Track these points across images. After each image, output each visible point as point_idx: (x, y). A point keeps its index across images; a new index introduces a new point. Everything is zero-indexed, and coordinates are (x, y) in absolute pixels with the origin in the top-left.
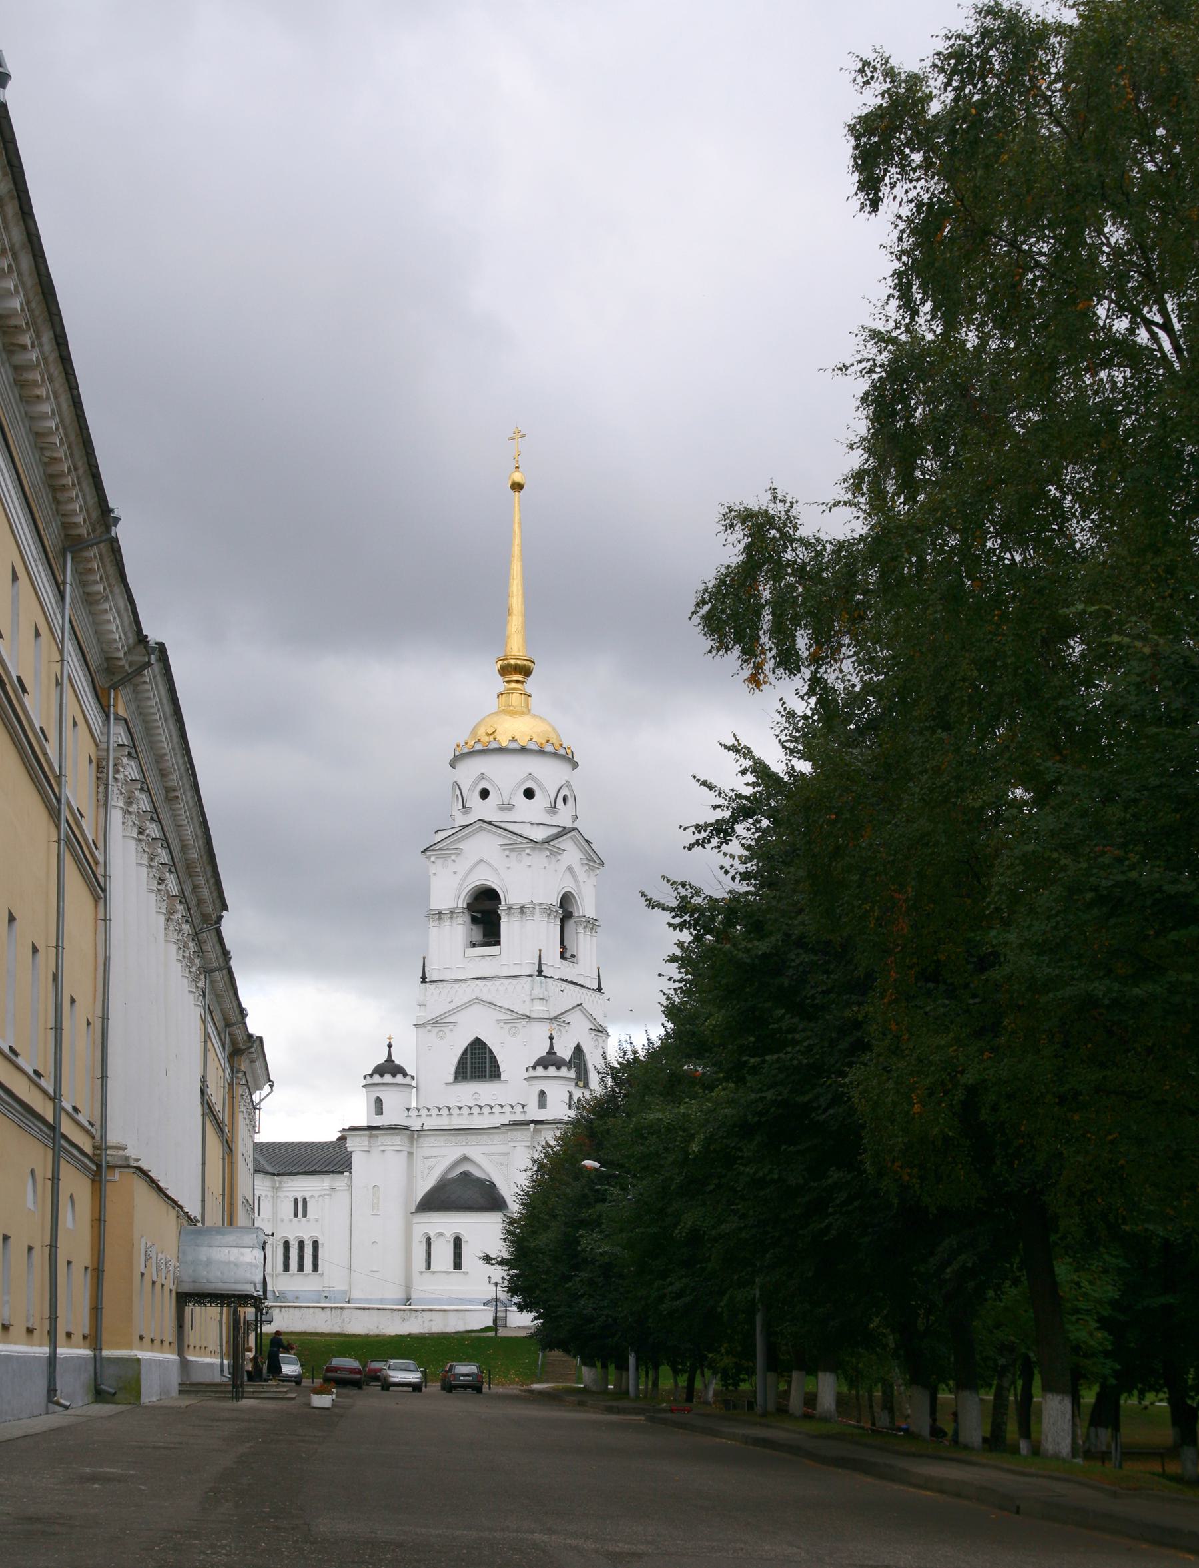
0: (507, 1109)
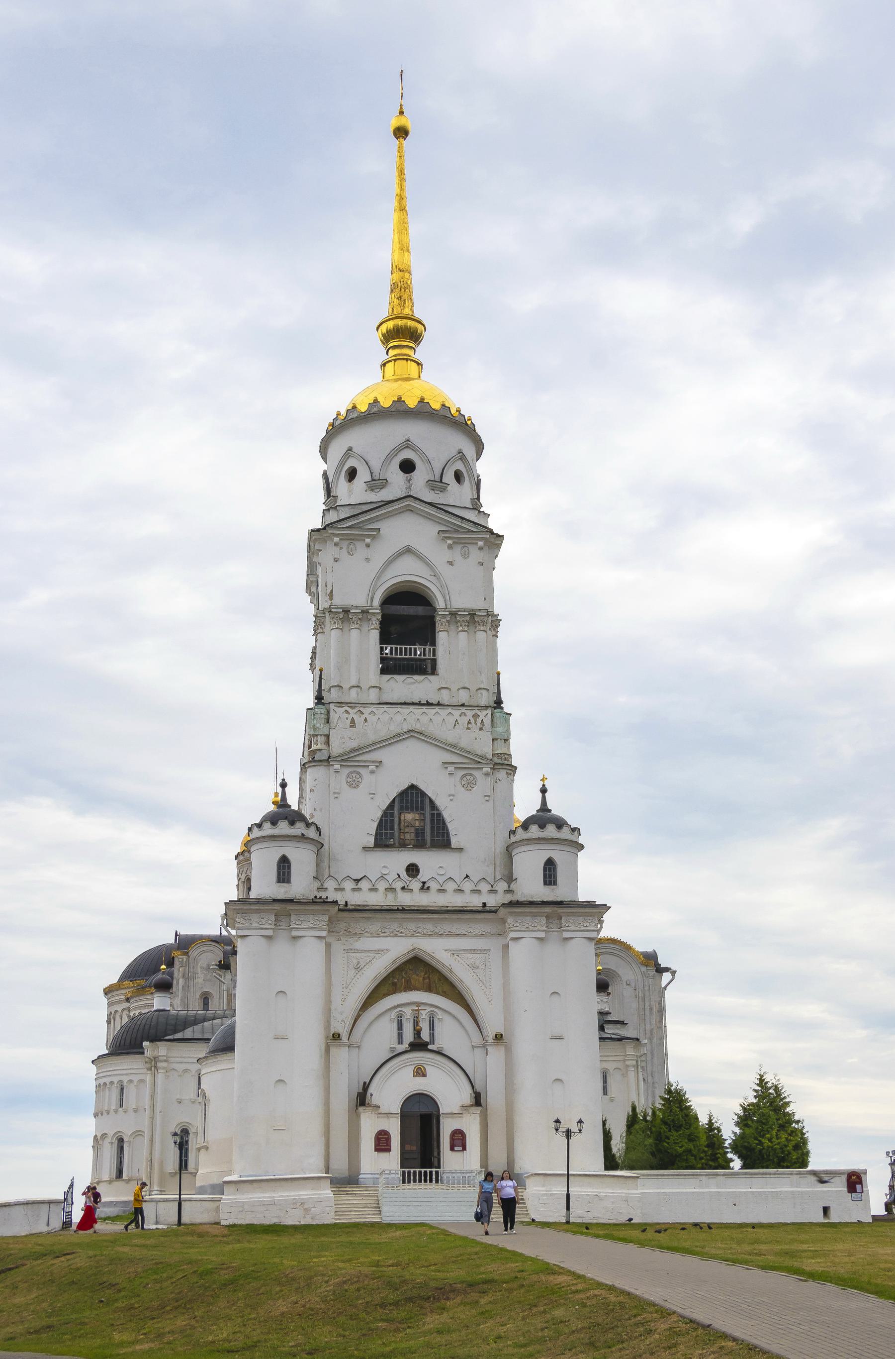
0: (484, 887)
